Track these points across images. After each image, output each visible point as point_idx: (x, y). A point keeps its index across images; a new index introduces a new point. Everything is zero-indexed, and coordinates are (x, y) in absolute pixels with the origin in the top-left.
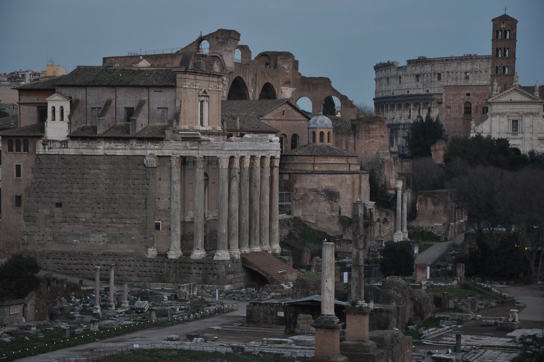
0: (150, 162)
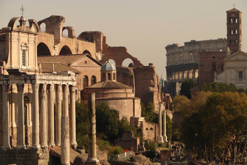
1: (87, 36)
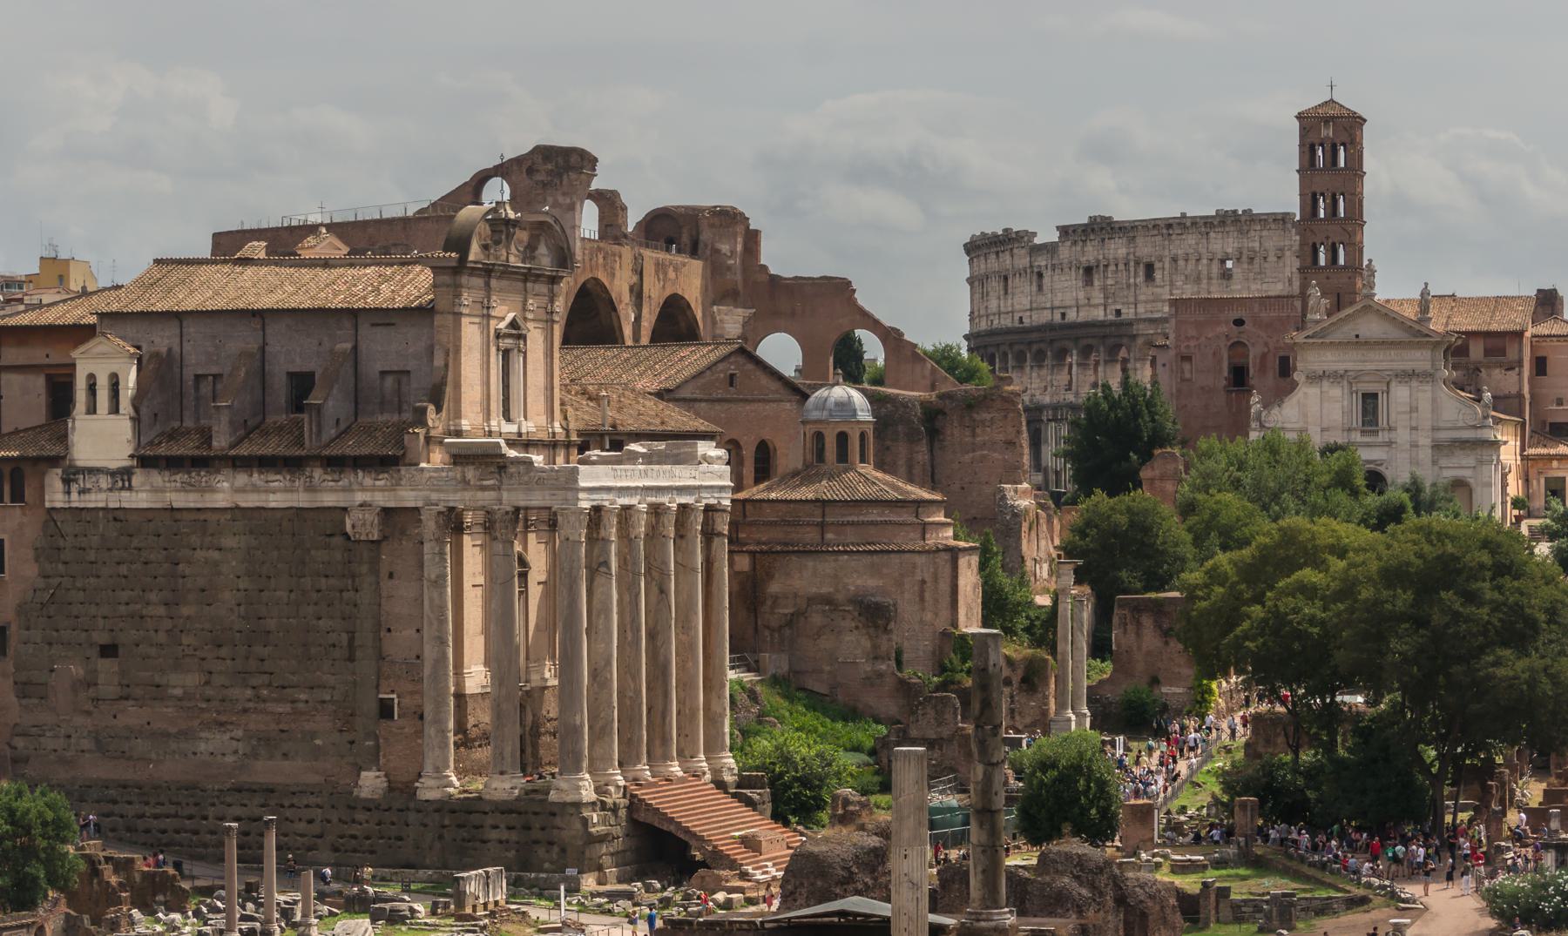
0: (362, 525)
1: (671, 229)
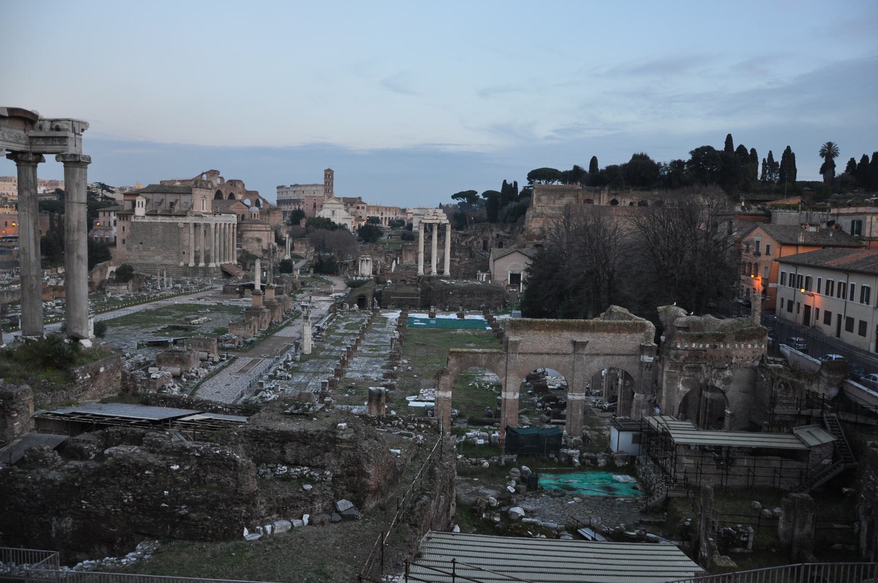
1: (232, 183)
